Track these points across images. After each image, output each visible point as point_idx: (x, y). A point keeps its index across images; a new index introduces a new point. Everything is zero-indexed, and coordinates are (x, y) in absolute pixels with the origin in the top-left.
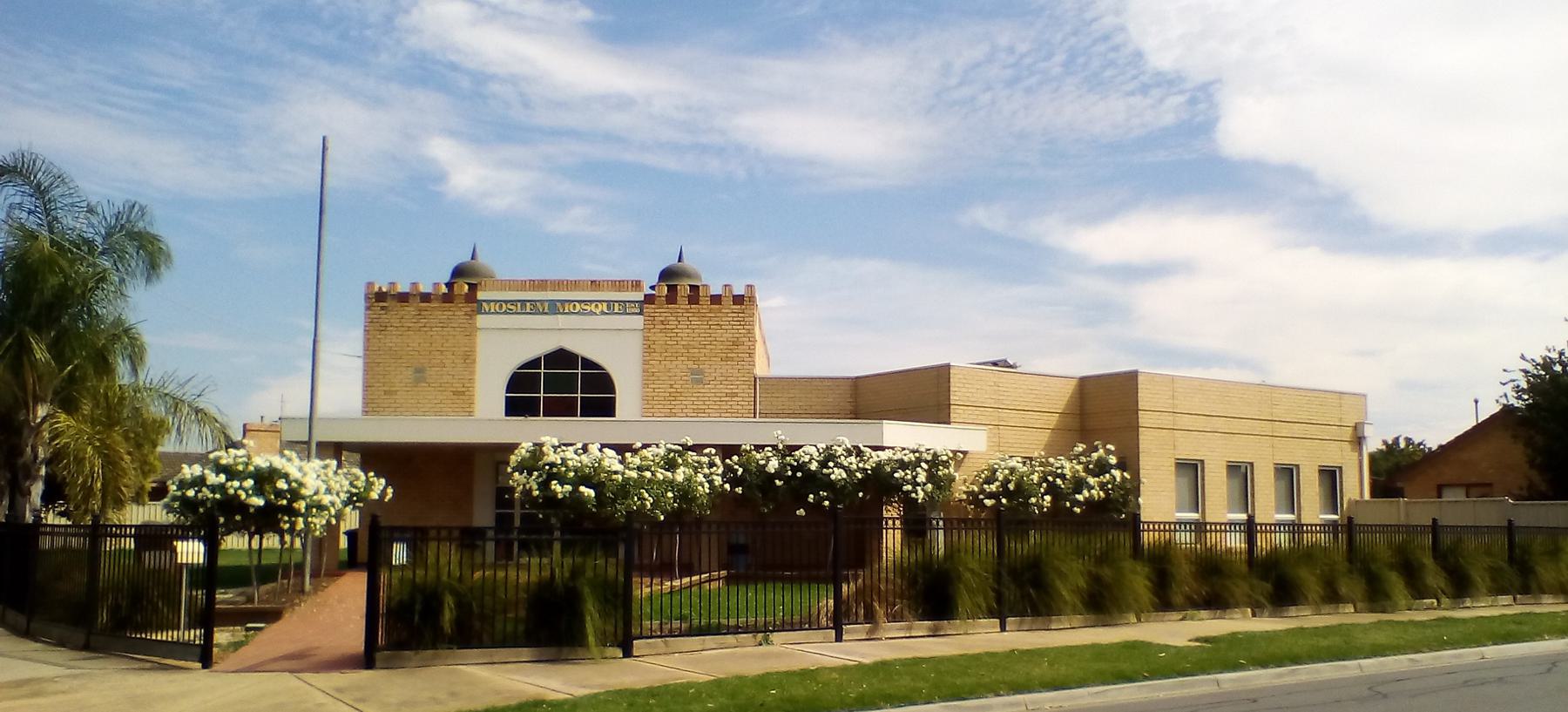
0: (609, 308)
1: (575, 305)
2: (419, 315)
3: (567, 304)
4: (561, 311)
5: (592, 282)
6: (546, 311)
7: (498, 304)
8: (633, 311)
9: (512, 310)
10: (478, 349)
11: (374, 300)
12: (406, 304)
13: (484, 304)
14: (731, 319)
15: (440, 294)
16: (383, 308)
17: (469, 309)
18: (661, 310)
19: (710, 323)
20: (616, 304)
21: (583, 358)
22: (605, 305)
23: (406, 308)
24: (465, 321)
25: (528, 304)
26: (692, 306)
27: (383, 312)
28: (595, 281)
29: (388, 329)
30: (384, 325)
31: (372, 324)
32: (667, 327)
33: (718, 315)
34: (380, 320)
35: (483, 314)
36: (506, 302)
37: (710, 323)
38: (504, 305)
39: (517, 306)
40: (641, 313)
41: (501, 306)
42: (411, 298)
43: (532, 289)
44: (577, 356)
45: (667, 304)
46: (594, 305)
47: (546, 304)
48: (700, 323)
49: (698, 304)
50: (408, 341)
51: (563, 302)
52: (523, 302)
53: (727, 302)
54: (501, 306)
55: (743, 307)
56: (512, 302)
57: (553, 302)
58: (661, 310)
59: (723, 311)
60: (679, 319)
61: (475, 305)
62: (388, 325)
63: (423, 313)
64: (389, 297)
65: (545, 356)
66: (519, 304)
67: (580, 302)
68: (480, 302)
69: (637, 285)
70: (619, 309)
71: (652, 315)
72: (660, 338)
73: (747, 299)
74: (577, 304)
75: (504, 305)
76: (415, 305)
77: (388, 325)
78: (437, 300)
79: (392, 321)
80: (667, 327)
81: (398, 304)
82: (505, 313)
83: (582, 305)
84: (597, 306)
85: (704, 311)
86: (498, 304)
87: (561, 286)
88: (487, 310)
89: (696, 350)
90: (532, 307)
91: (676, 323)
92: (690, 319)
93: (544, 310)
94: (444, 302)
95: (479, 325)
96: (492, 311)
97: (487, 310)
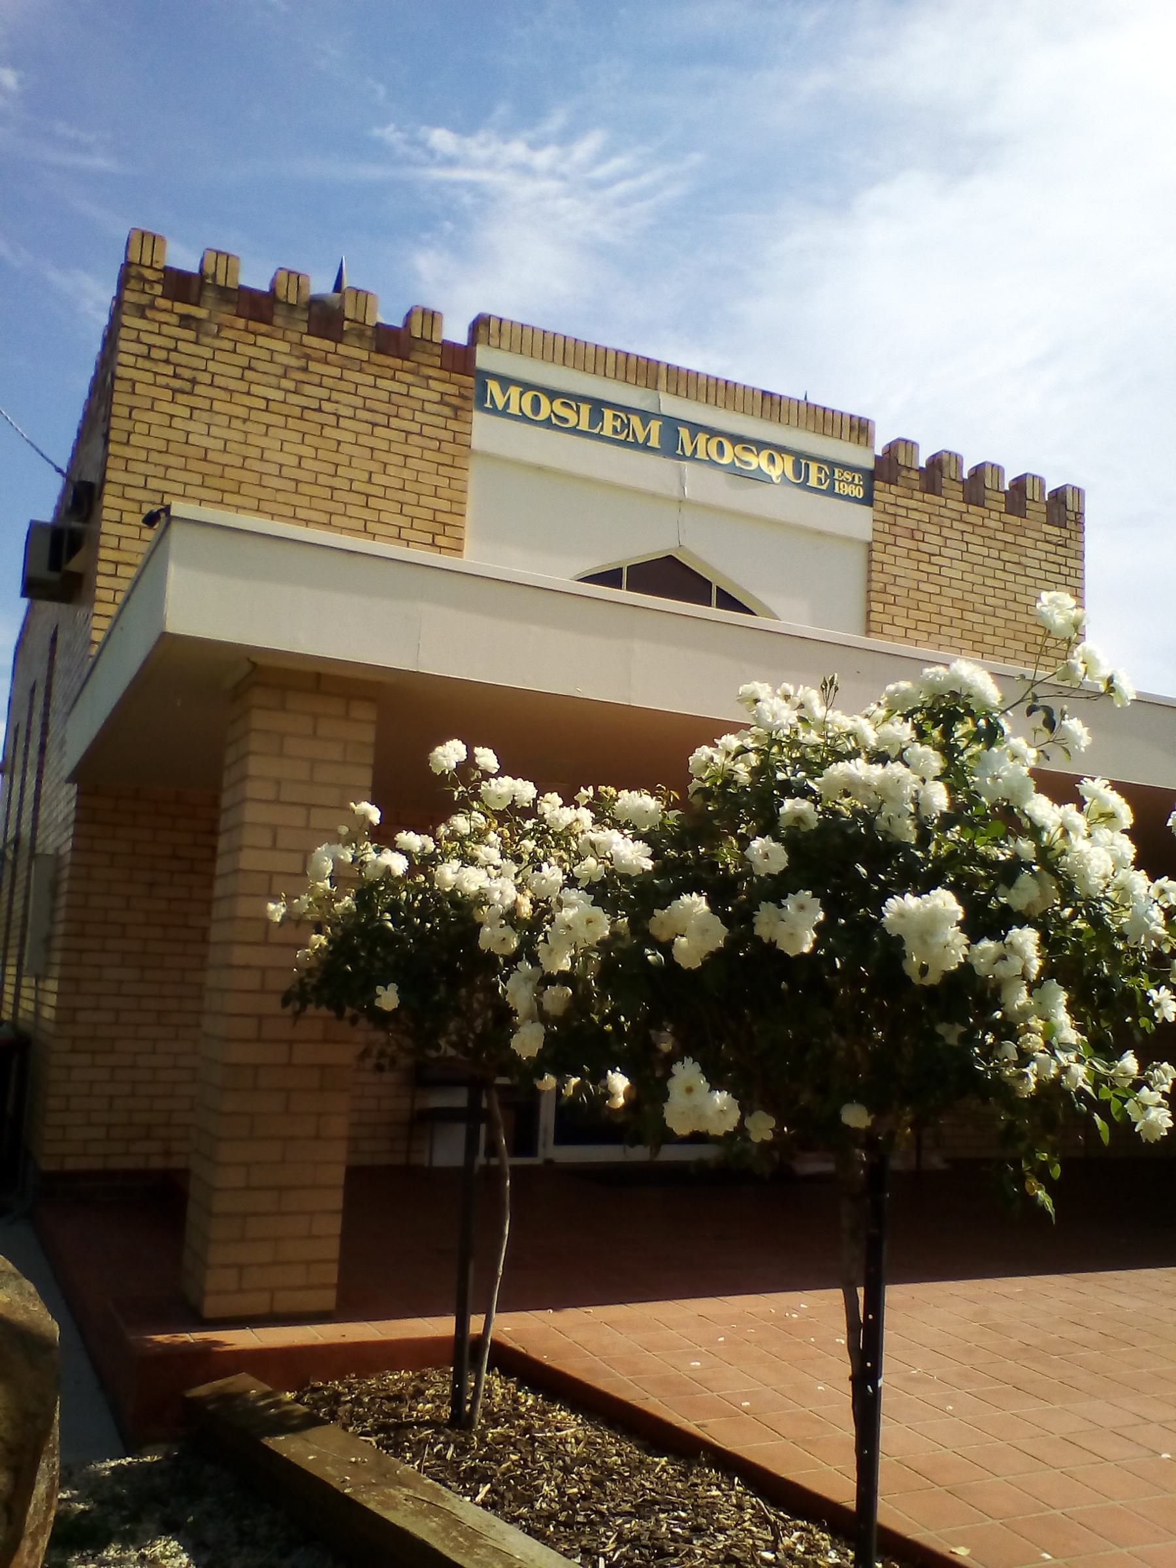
0: (797, 474)
1: (720, 446)
2: (305, 370)
3: (702, 438)
4: (688, 453)
5: (764, 393)
6: (654, 442)
7: (529, 396)
8: (849, 490)
9: (566, 420)
10: (469, 510)
11: (158, 289)
12: (263, 328)
13: (493, 387)
14: (1043, 556)
15: (370, 322)
16: (186, 321)
17: (453, 389)
18: (912, 504)
19: (1005, 556)
20: (813, 467)
21: (717, 587)
22: (789, 461)
23: (261, 340)
24: (440, 421)
25: (608, 414)
26: (972, 508)
27: (190, 335)
28: (771, 394)
29: (199, 389)
30: (187, 373)
31: (147, 364)
32: (922, 546)
33: (1020, 540)
34: (174, 356)
35: (487, 410)
36: (553, 394)
37: (1005, 556)
38: (544, 401)
39: (578, 412)
40: (868, 500)
41: (536, 405)
42: (280, 310)
43: (621, 374)
44: (709, 584)
45: (924, 491)
46: (765, 454)
47: (655, 425)
48: (985, 551)
49: (983, 506)
50: (264, 442)
51: (696, 428)
52: (598, 406)
53: (1037, 511)
54: (536, 405)
55: (1065, 533)
56: (573, 399)
57: (672, 424)
58: (912, 504)
59: (1029, 533)
60: (946, 532)
61: (469, 381)
62: (206, 378)
63: (313, 366)
64: (209, 294)
65: (628, 567)
66: (585, 409)
67: (736, 439)
68: (483, 377)
69: (860, 429)
70: (819, 479)
71: (891, 510)
72: (904, 567)
73: (1071, 516)
74: (727, 446)
75: (544, 401)
76: (293, 337)
77: (206, 378)
78: (361, 335)
79: (212, 367)
80: (922, 546)
81: (241, 322)
82: (547, 423)
83: (738, 448)
84: (772, 460)
85: (993, 524)
86: (529, 396)
87: (692, 391)
88: (500, 406)
89: (979, 618)
90: (618, 424)
91: (939, 541)
92: (967, 537)
93: (648, 438)
94: (379, 351)
95: (476, 442)
96: (514, 409)
97: (500, 406)
